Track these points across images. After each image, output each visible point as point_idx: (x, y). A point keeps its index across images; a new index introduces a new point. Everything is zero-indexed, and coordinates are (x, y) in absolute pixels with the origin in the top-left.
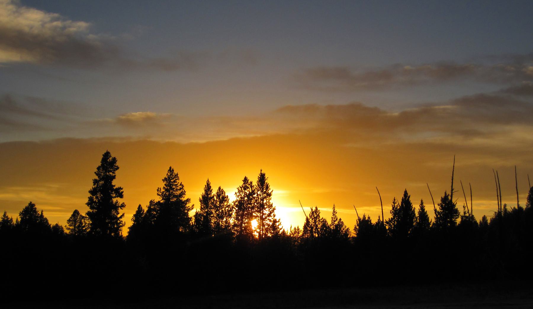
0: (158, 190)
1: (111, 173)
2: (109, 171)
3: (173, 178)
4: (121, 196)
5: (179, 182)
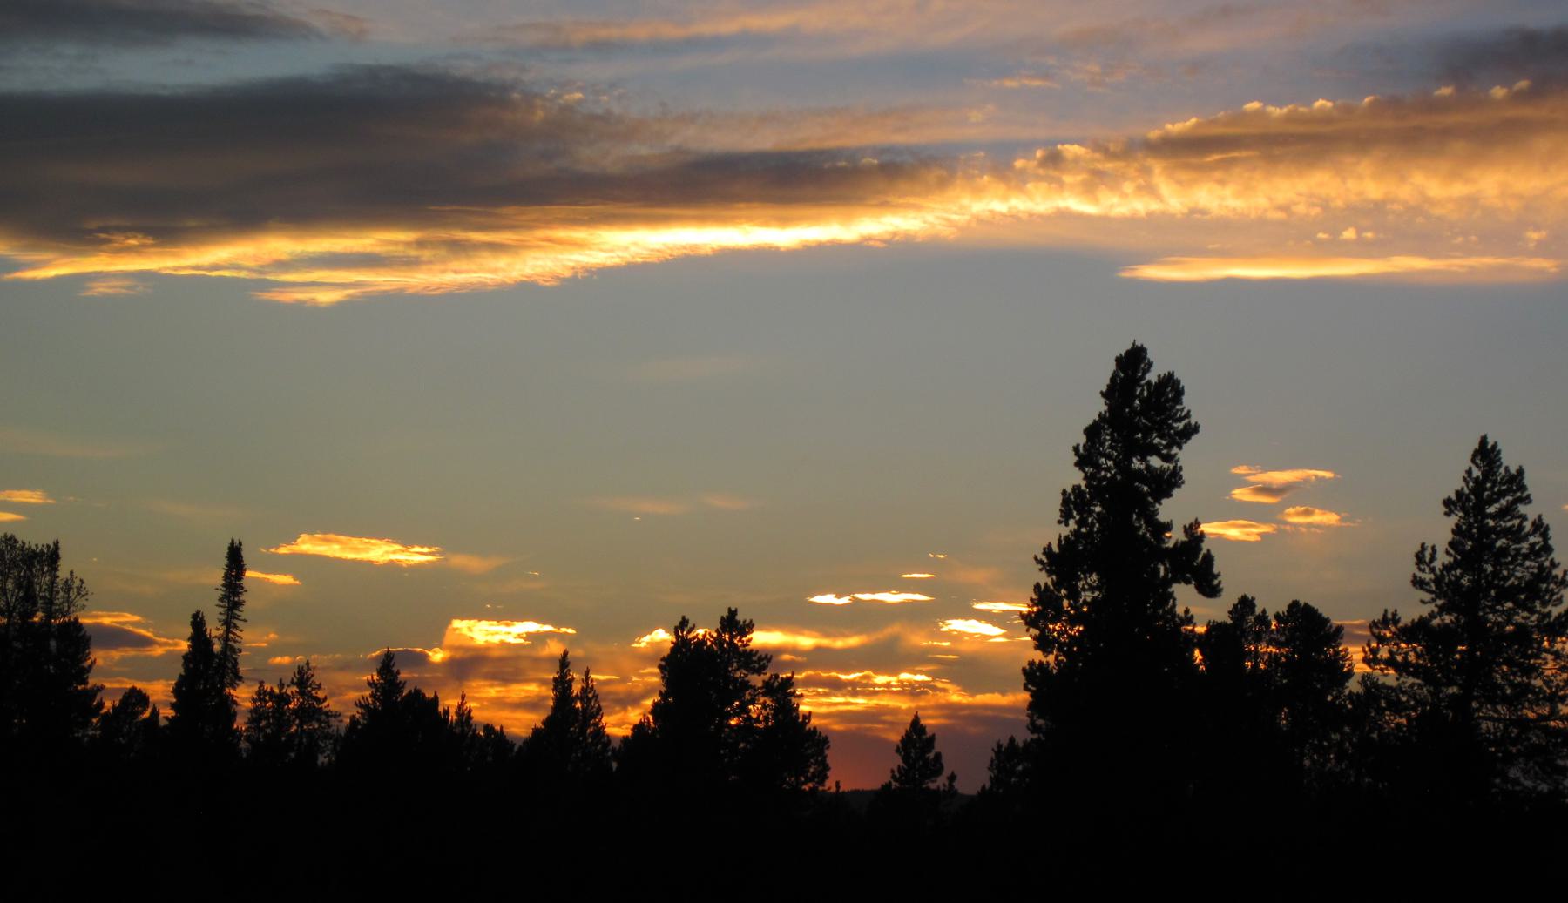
0: (1420, 558)
1: (1155, 462)
2: (1148, 450)
3: (1502, 494)
4: (1209, 588)
5: (1529, 511)
